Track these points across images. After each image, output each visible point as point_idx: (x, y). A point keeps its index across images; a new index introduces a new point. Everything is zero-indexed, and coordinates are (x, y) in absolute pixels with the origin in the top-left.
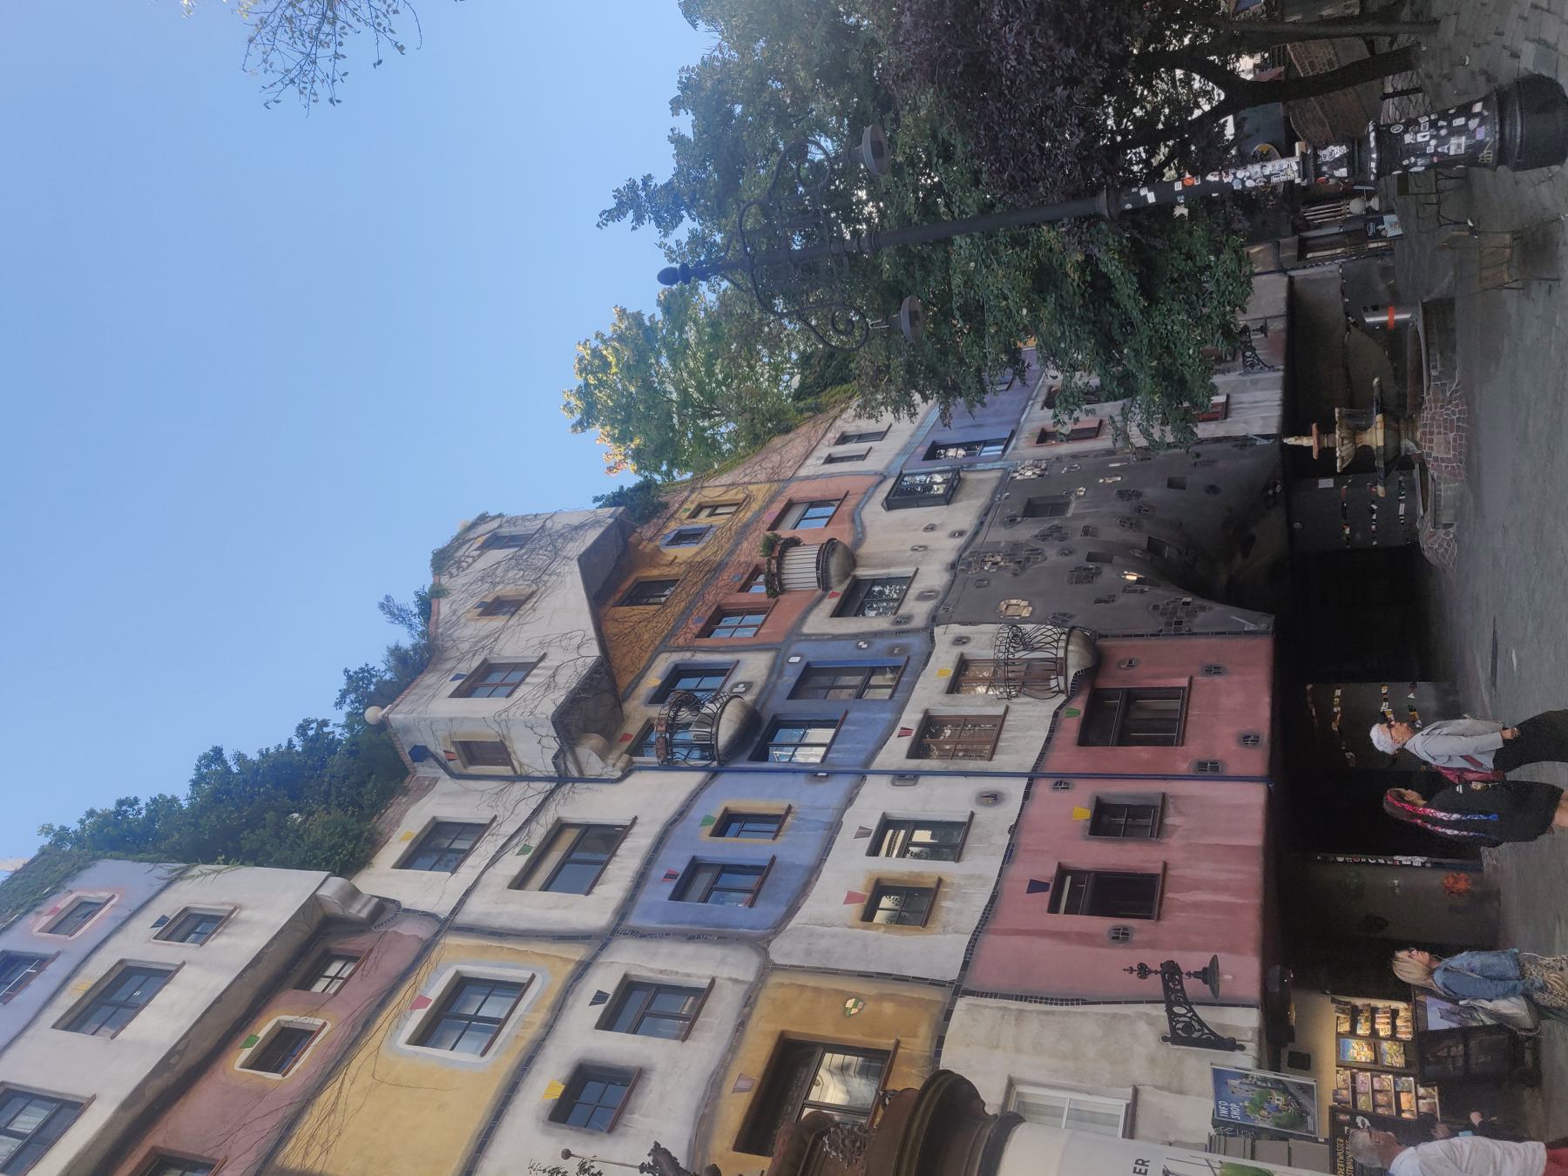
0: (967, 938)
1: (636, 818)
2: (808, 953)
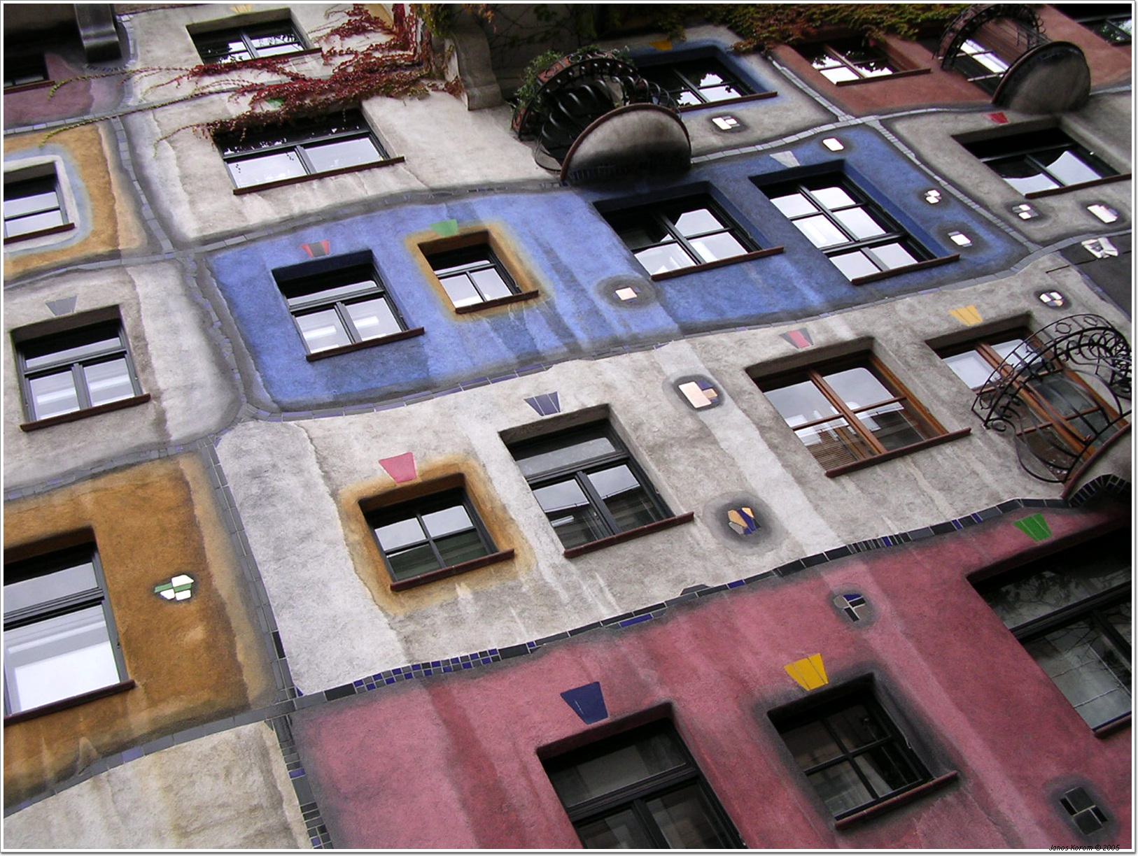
0: (402, 663)
1: (401, 160)
2: (256, 474)
